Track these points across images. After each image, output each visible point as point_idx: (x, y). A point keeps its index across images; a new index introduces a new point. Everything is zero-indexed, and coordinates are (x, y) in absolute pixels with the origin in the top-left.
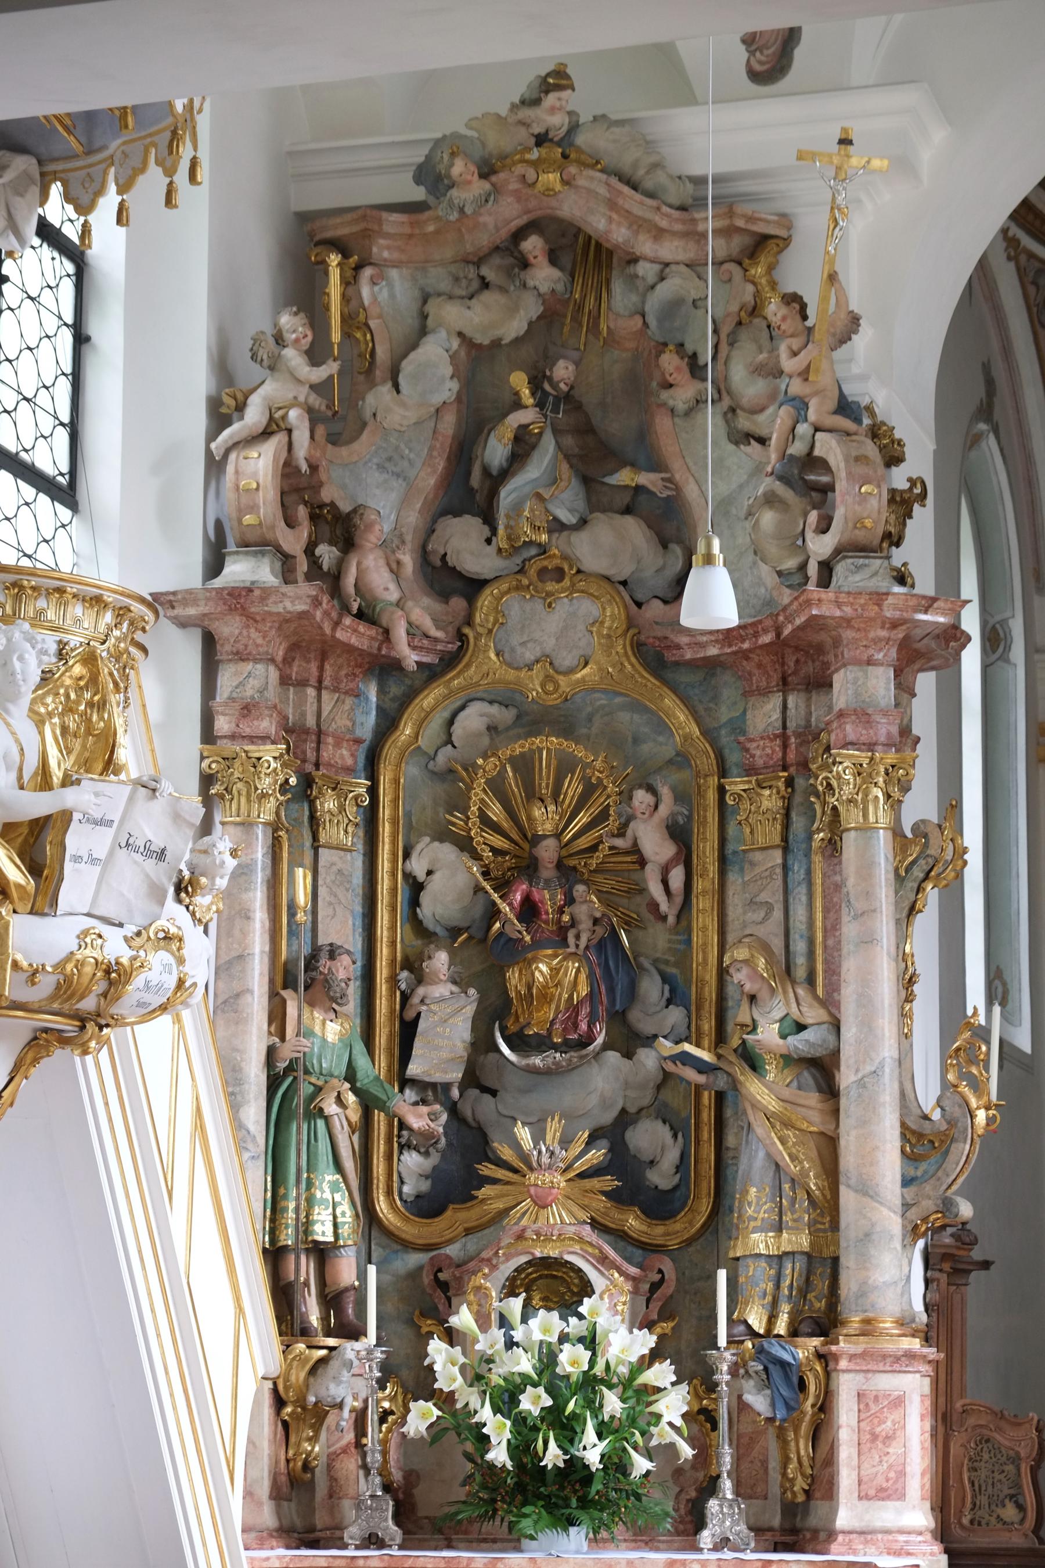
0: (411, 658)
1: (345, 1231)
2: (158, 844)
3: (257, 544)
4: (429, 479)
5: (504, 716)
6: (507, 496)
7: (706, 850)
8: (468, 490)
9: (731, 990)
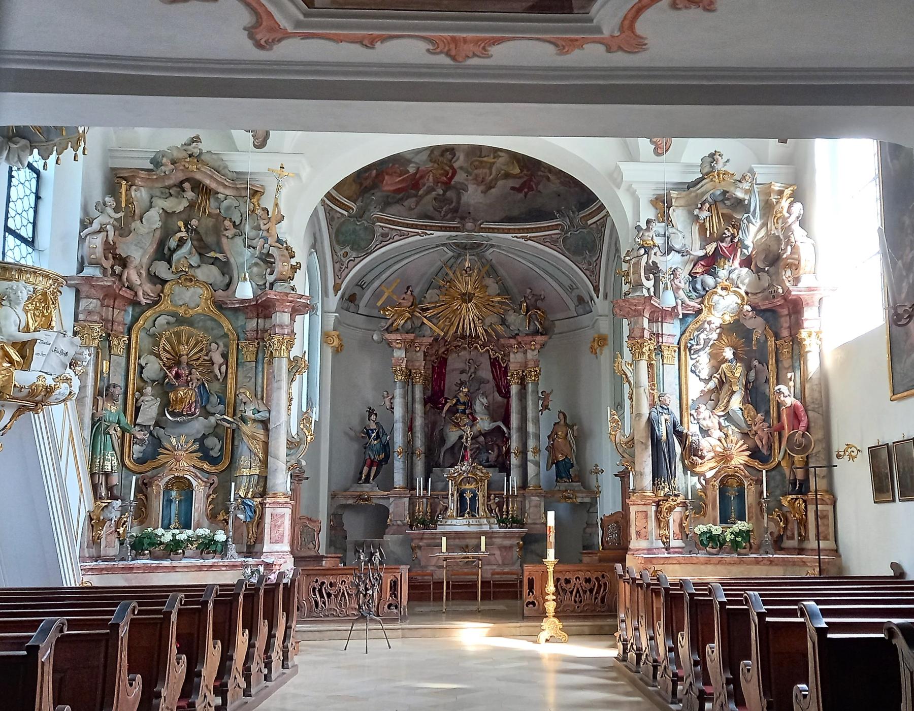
0: (144, 301)
1: (115, 468)
2: (65, 351)
3: (95, 263)
4: (151, 249)
5: (172, 320)
7: (232, 360)
8: (163, 253)
9: (238, 401)
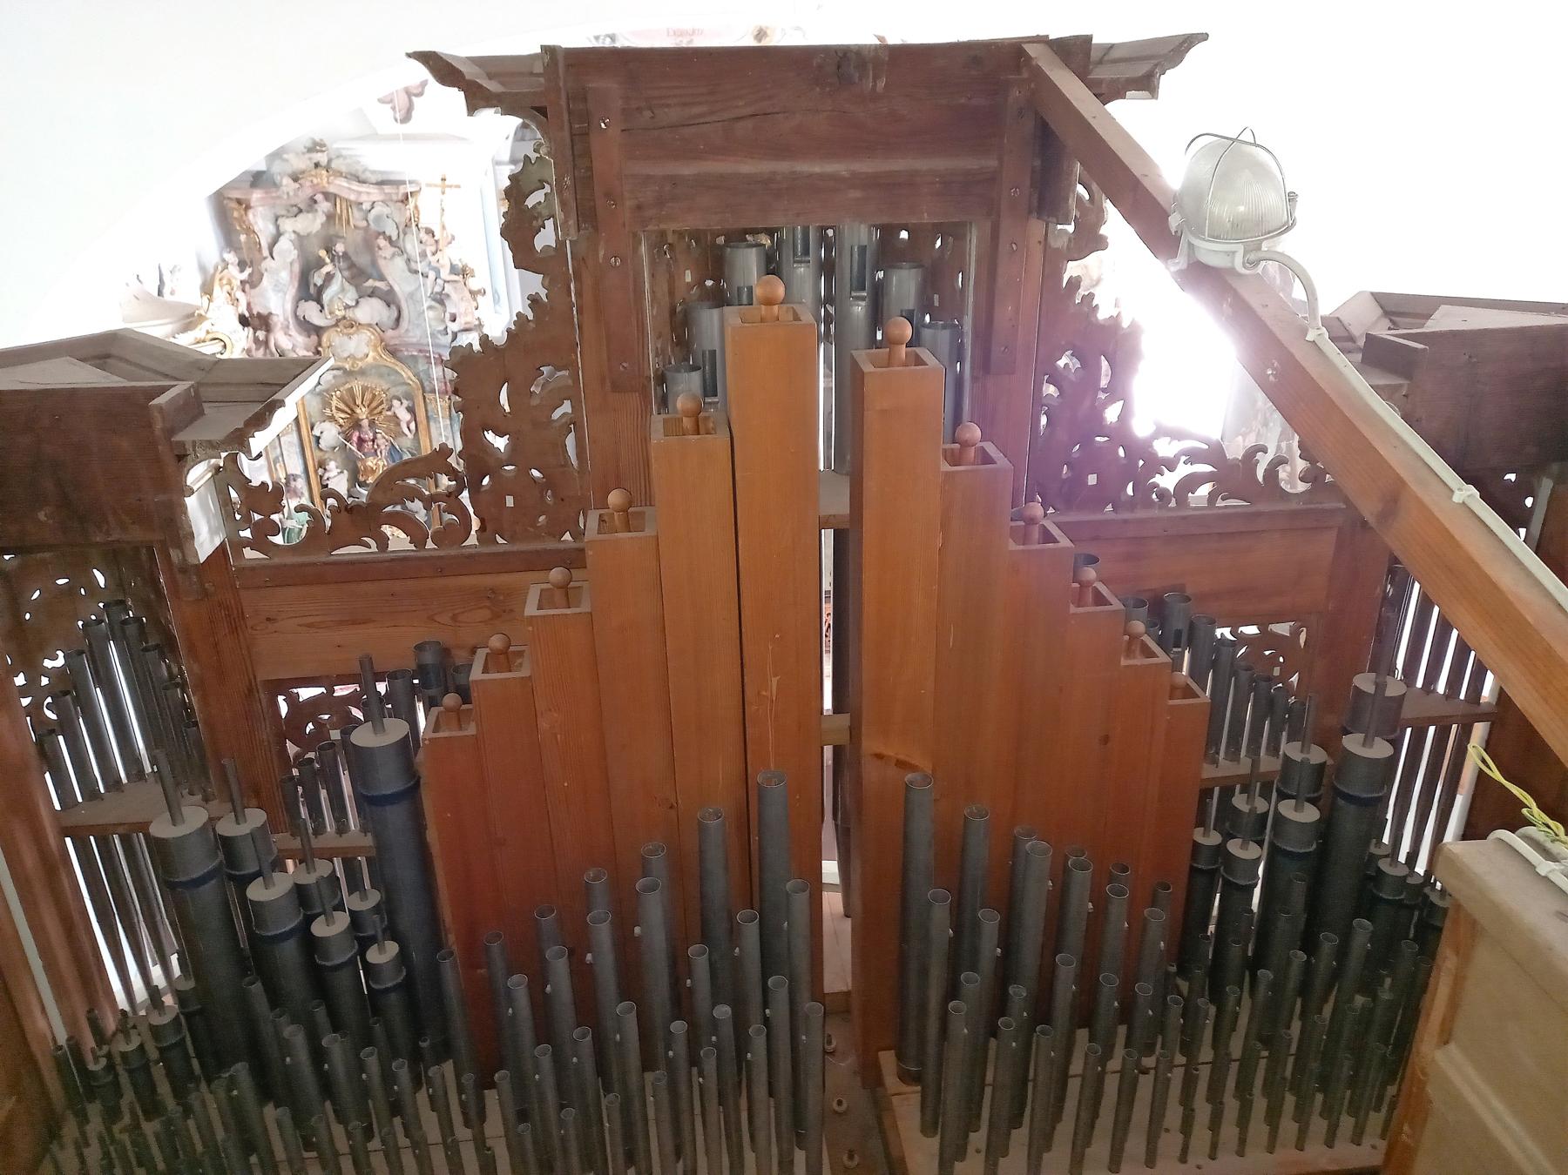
4: (292, 291)
6: (326, 297)
8: (308, 291)
